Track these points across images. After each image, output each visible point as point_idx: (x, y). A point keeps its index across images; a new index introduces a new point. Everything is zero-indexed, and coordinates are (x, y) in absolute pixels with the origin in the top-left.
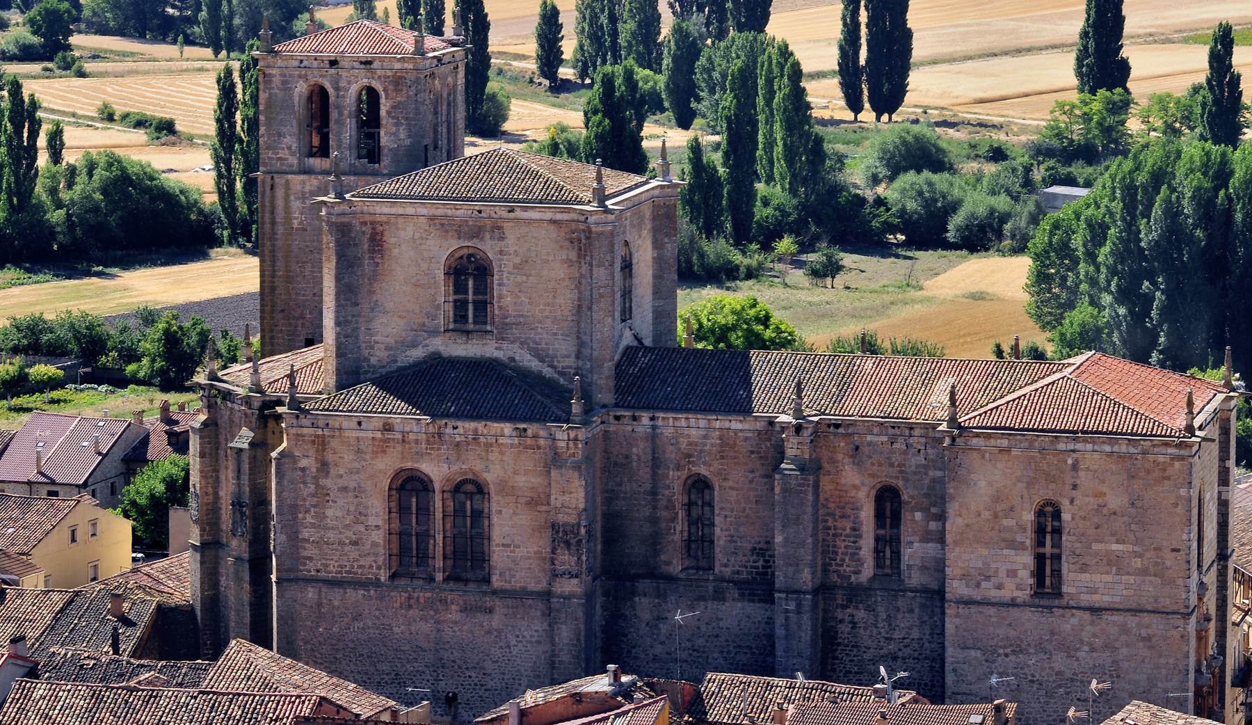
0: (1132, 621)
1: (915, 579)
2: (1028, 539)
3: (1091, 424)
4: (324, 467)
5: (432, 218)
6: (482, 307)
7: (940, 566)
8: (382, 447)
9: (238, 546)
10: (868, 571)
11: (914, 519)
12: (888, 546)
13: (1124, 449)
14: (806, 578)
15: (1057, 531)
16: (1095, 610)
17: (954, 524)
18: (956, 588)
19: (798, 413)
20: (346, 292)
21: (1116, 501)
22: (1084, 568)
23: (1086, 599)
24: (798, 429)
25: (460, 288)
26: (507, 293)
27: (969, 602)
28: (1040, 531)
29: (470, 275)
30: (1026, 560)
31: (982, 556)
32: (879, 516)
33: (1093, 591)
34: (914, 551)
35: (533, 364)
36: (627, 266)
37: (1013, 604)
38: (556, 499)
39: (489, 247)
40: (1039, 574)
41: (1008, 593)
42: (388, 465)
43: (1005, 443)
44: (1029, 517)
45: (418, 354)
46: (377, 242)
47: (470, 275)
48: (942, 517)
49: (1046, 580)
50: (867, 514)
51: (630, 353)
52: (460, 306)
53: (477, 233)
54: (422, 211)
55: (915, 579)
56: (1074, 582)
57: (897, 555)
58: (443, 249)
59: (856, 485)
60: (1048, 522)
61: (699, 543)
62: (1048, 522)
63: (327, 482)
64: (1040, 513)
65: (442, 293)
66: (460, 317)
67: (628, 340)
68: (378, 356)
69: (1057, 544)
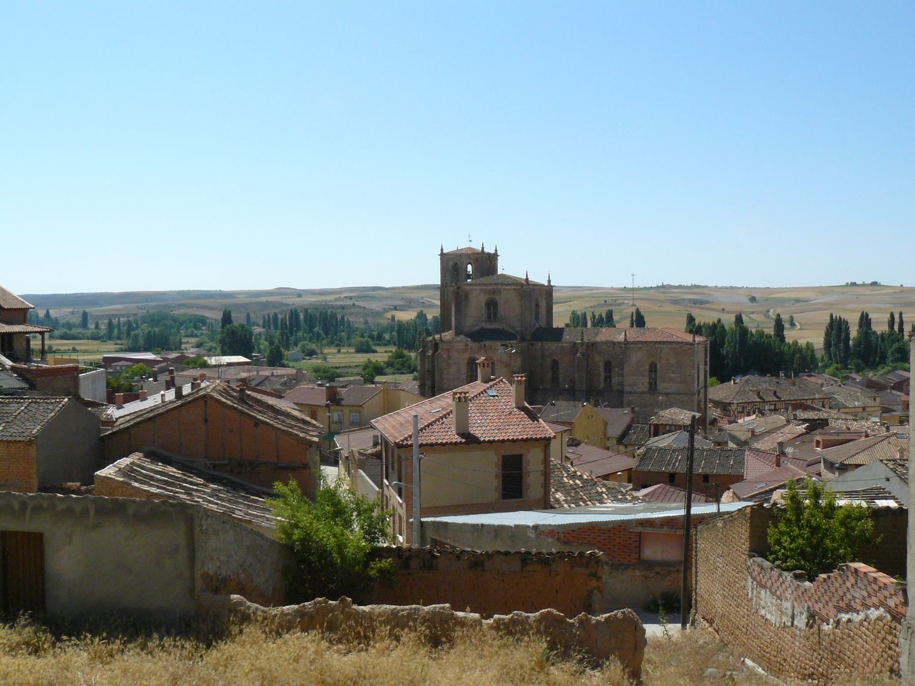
0: (677, 397)
1: (616, 388)
2: (647, 373)
3: (665, 340)
4: (449, 357)
5: (481, 290)
6: (495, 314)
7: (622, 384)
8: (465, 351)
9: (428, 383)
10: (602, 386)
11: (615, 370)
12: (608, 378)
13: (674, 346)
14: (584, 387)
15: (656, 371)
16: (667, 394)
17: (627, 369)
18: (627, 388)
19: (582, 339)
20: (458, 311)
21: (672, 361)
22: (664, 382)
23: (664, 391)
24: (582, 344)
25: (489, 309)
26: (502, 310)
27: (630, 393)
28: (651, 371)
29: (492, 305)
30: (647, 380)
31: (634, 380)
32: (606, 370)
33: (666, 388)
34: (615, 380)
35: (509, 329)
36: (537, 305)
37: (643, 393)
38: (513, 364)
39: (497, 297)
40: (650, 384)
41: (640, 390)
42: (466, 356)
43: (640, 345)
44: (647, 367)
45: (477, 328)
46: (467, 297)
47: (492, 305)
48: (622, 370)
49: (653, 387)
50: (602, 369)
51: (538, 329)
52: (489, 314)
53: (493, 293)
54: (479, 287)
55: (616, 388)
56: (661, 386)
57: (610, 381)
58: (483, 299)
59: (599, 360)
60: (653, 368)
61: (555, 379)
62: (653, 368)
63: (451, 362)
64: (650, 366)
65: (484, 310)
66: (489, 317)
67: (537, 326)
68: (467, 329)
69: (656, 375)
